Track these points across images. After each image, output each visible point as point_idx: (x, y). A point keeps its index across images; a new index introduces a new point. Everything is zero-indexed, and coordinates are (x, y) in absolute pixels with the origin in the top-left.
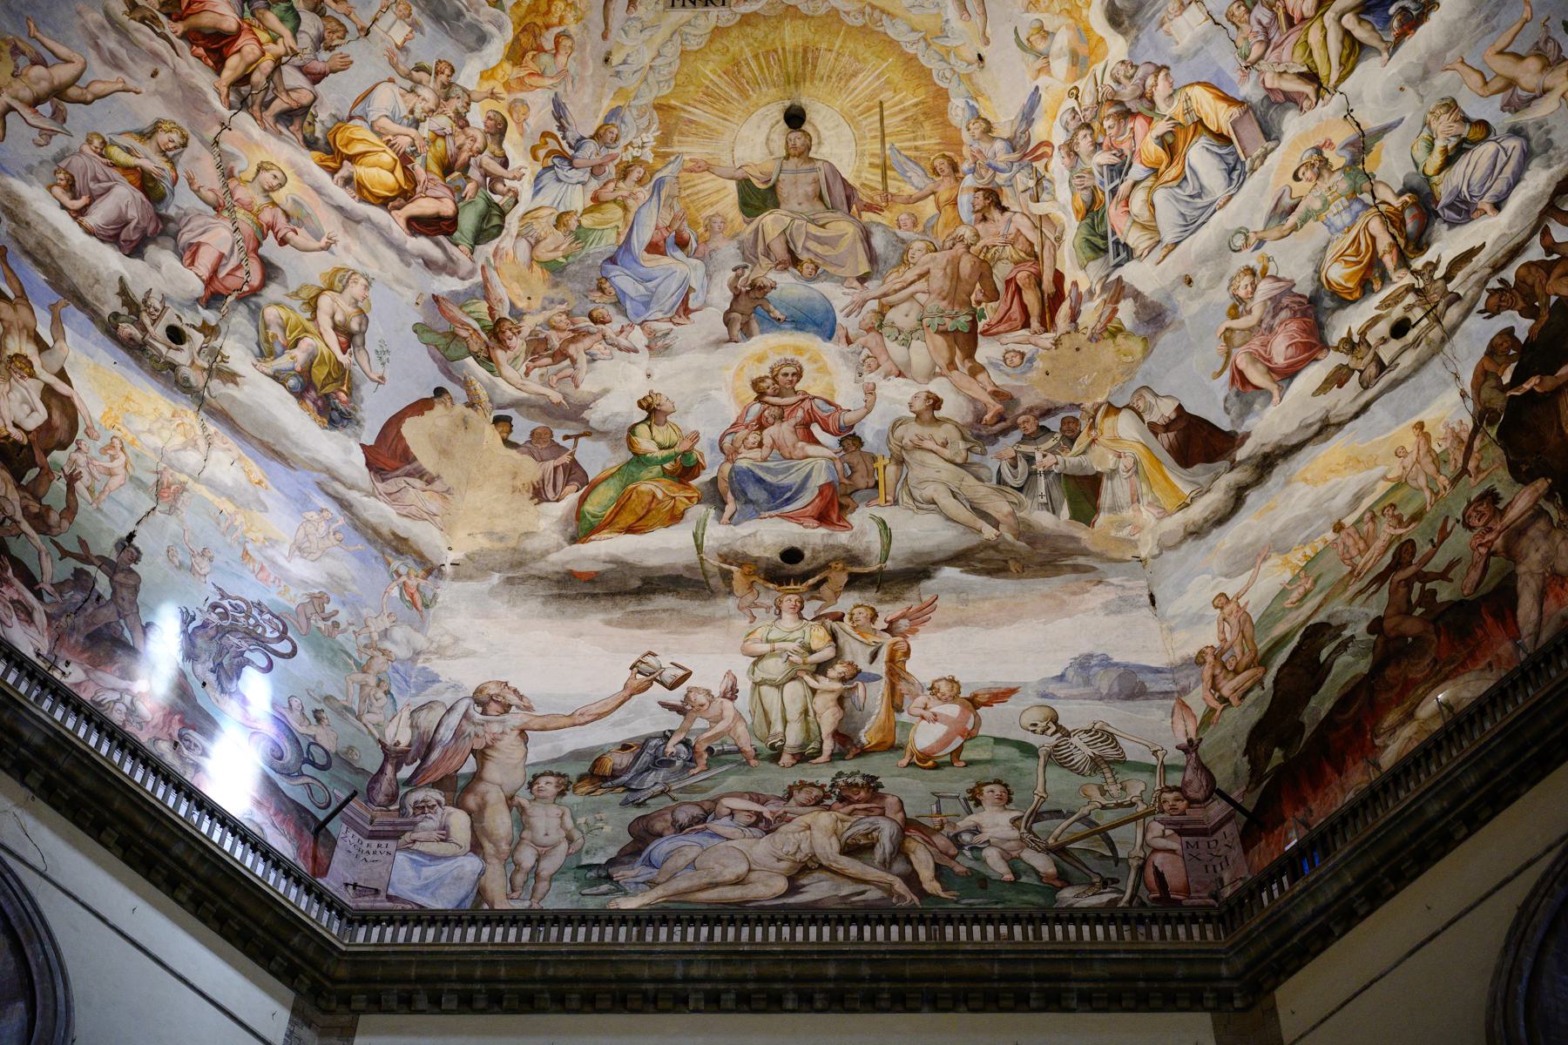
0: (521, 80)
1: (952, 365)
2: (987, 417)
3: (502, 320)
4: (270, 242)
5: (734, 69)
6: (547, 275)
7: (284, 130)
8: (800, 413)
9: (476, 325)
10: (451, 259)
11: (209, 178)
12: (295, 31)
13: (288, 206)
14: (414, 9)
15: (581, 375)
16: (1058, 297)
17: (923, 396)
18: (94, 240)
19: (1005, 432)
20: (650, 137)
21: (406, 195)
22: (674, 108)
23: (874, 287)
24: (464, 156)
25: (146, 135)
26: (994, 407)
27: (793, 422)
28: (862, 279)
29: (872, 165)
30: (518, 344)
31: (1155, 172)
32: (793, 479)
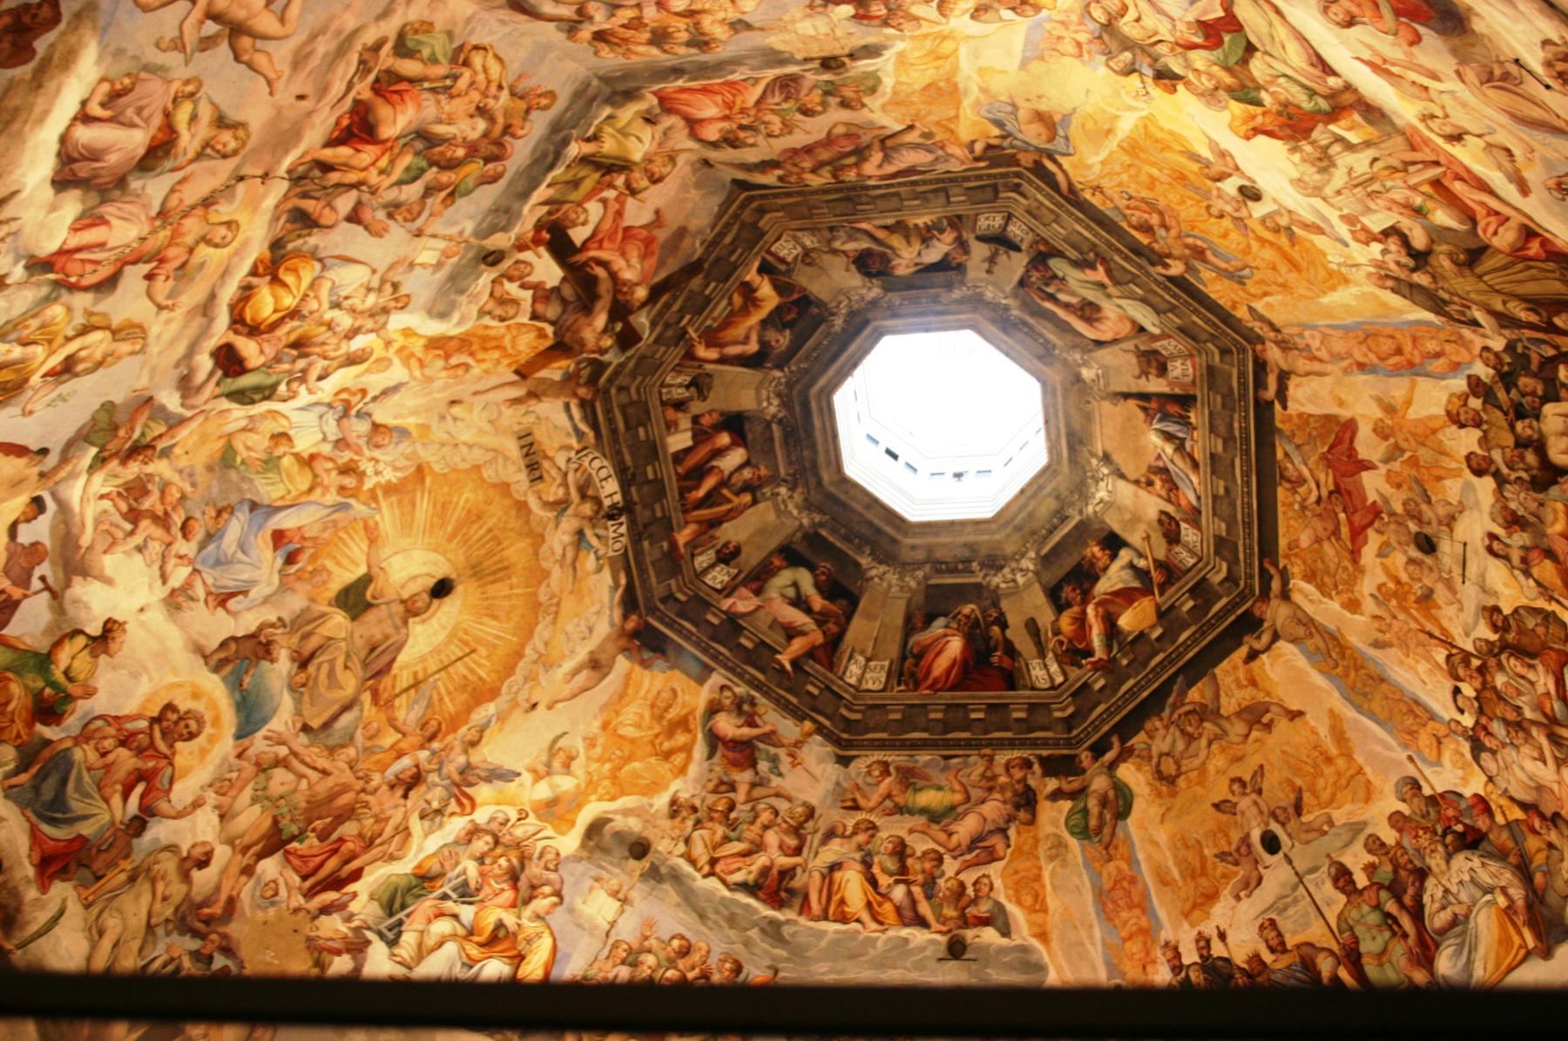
0: (412, 355)
1: (247, 848)
2: (206, 911)
3: (154, 448)
4: (145, 268)
5: (474, 516)
6: (219, 455)
7: (284, 218)
8: (151, 764)
9: (136, 435)
10: (200, 388)
11: (193, 193)
12: (400, 183)
13: (196, 259)
14: (455, 259)
15: (119, 549)
16: (337, 883)
17: (208, 848)
18: (54, 146)
19: (196, 934)
20: (389, 475)
21: (254, 330)
22: (422, 480)
23: (303, 739)
24: (317, 350)
25: (221, 122)
26: (217, 909)
27: (139, 764)
28: (306, 728)
29: (415, 674)
30: (134, 469)
31: (471, 932)
32: (77, 806)
